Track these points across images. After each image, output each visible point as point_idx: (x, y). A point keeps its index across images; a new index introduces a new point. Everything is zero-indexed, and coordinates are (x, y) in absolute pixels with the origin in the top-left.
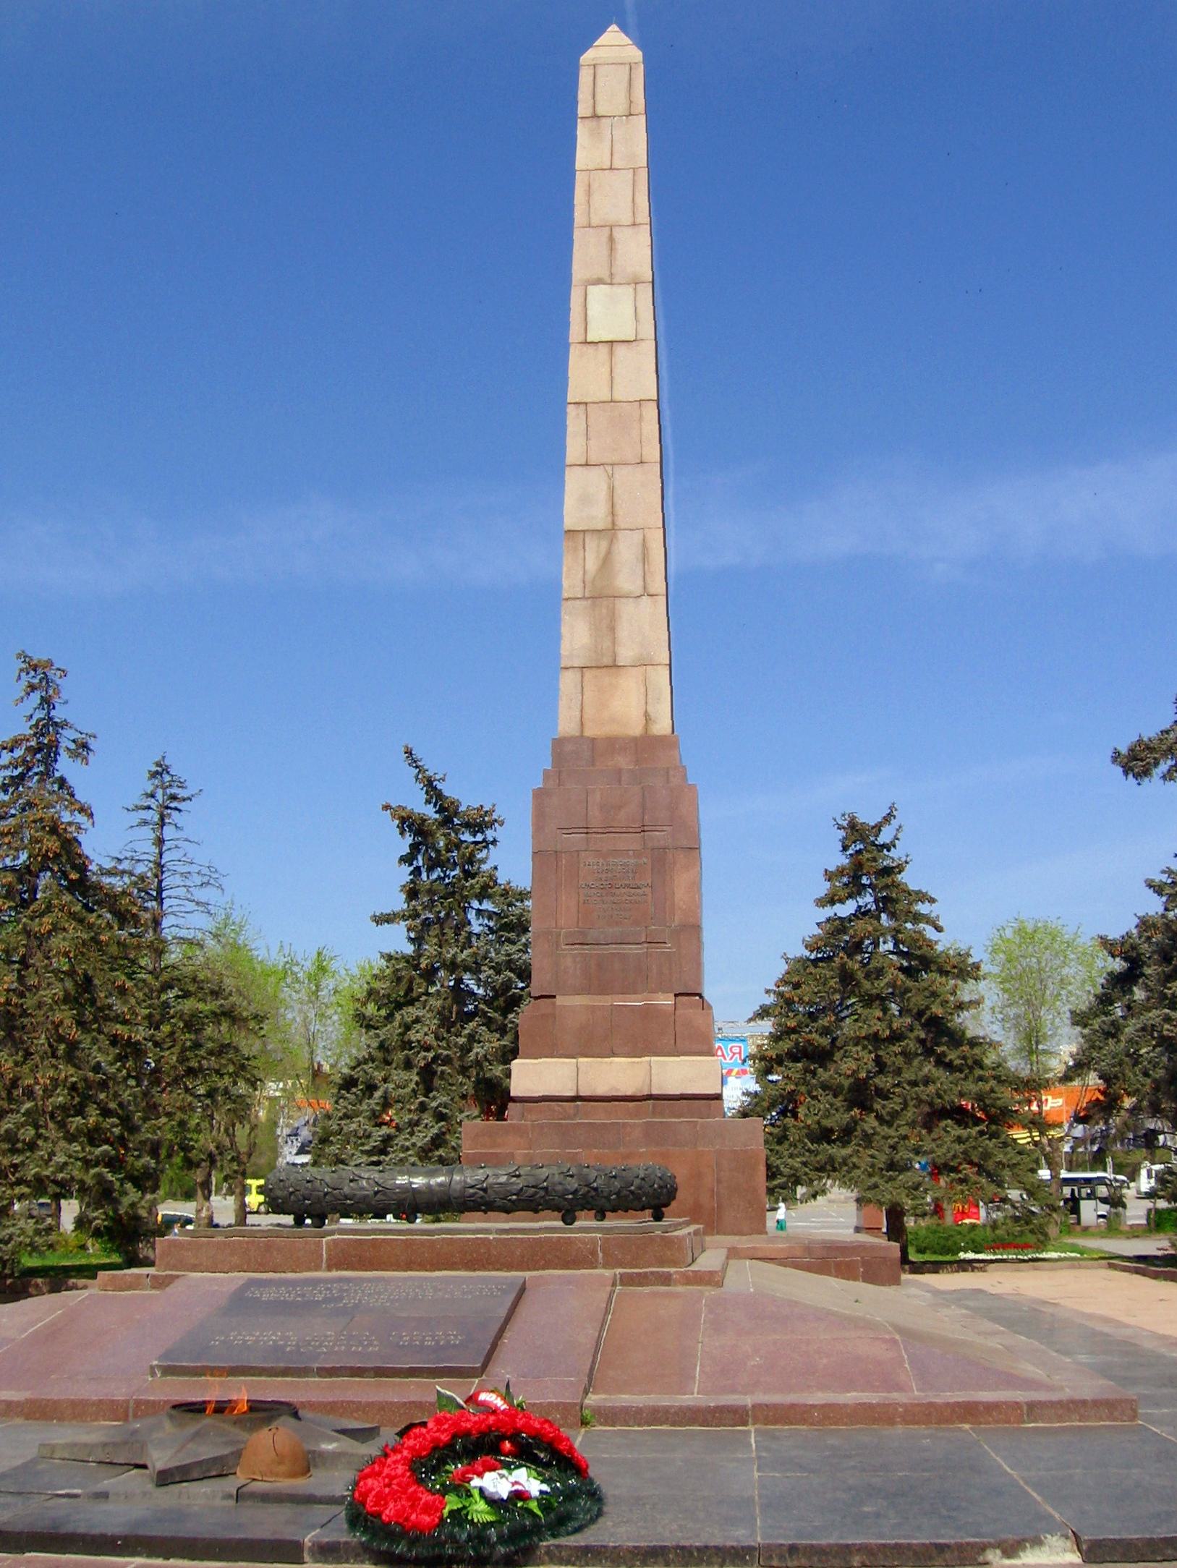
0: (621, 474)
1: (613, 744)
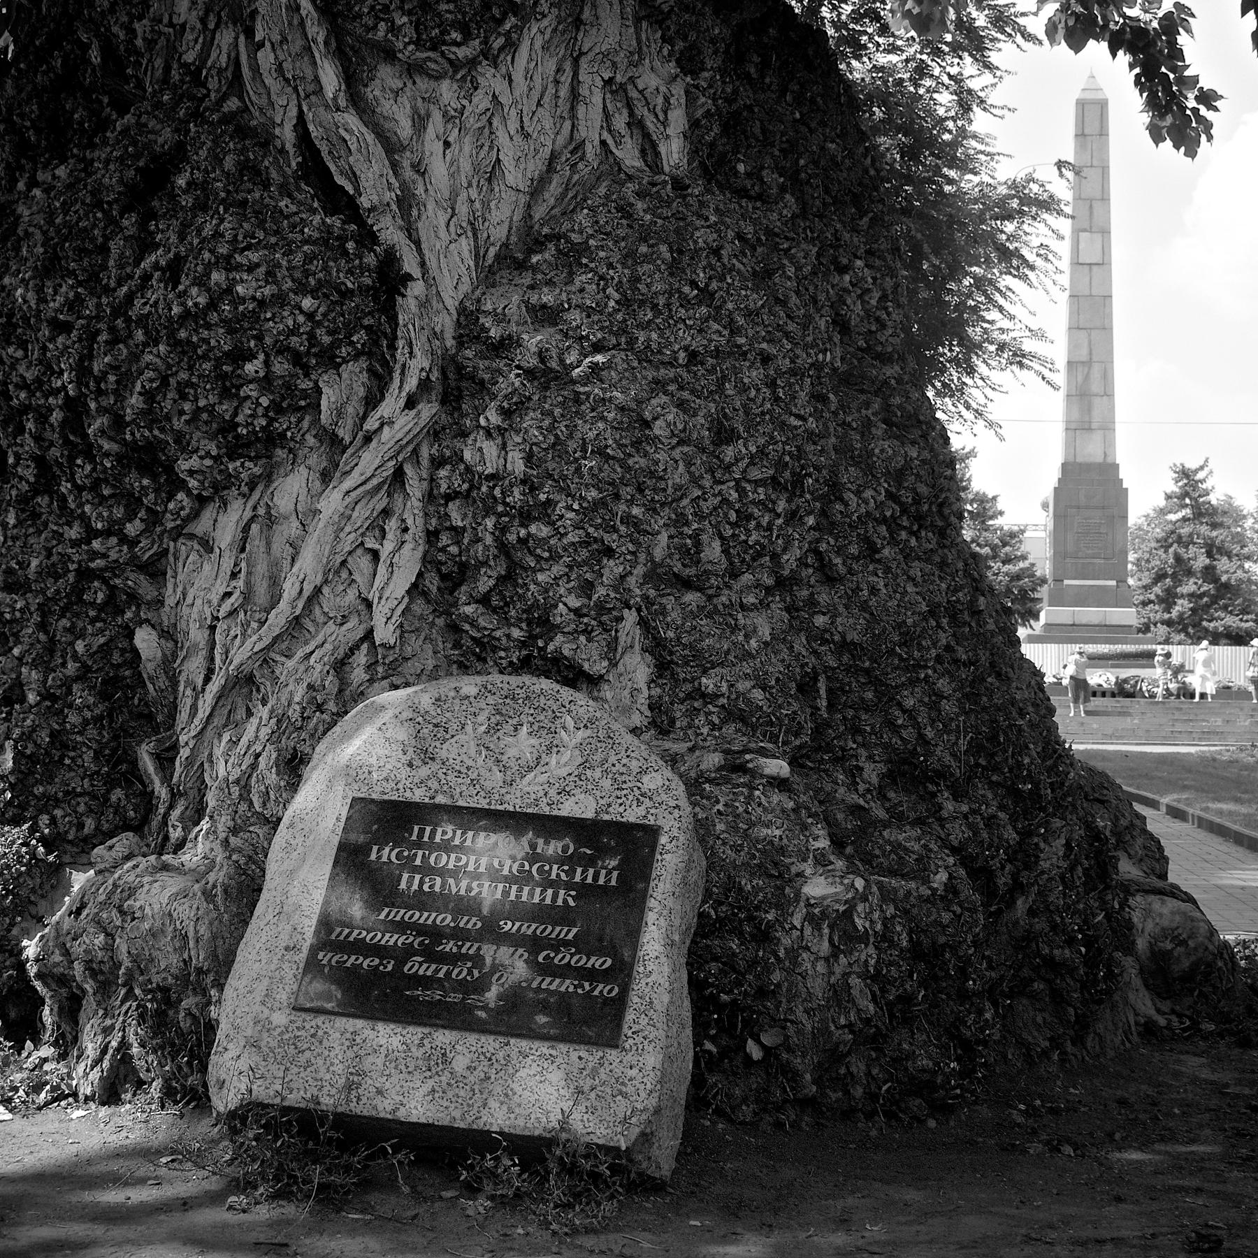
0: (1093, 333)
1: (1087, 467)
